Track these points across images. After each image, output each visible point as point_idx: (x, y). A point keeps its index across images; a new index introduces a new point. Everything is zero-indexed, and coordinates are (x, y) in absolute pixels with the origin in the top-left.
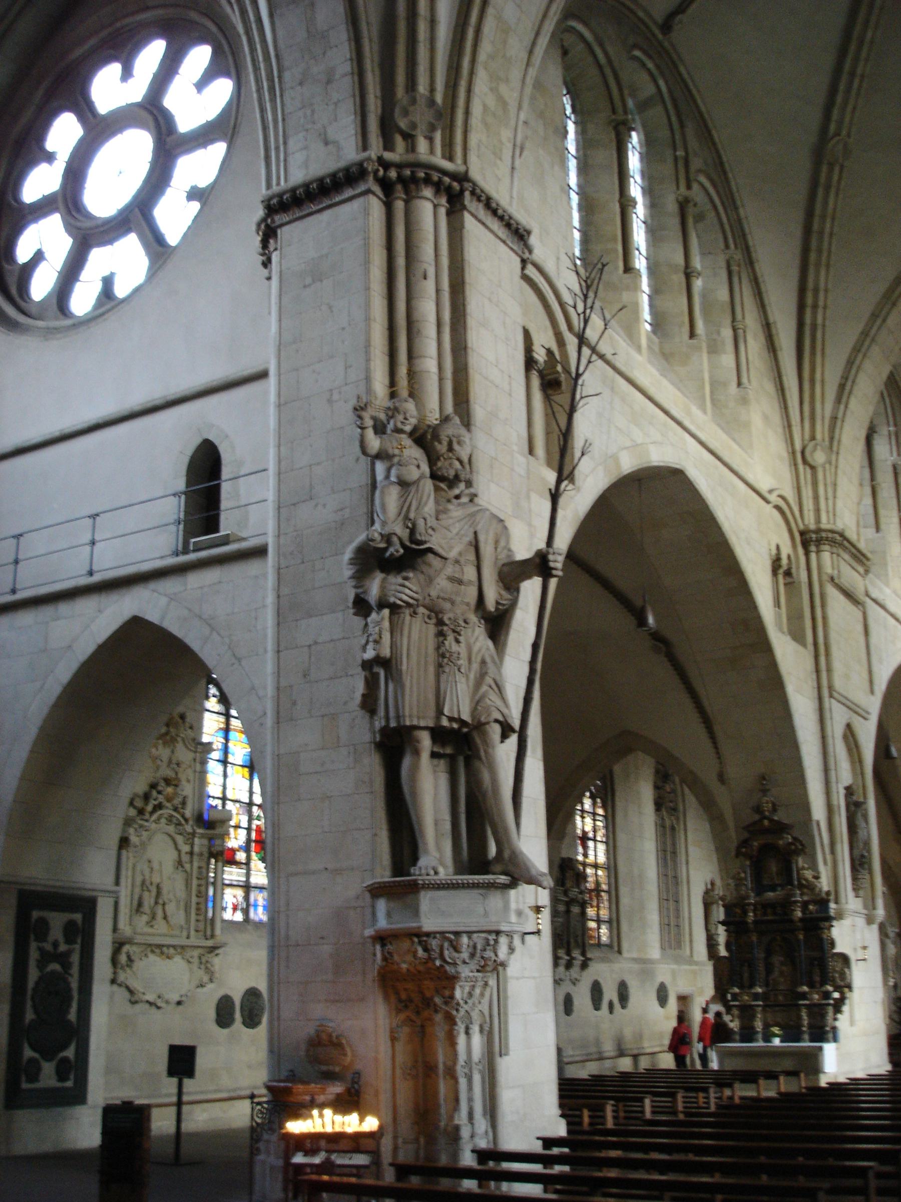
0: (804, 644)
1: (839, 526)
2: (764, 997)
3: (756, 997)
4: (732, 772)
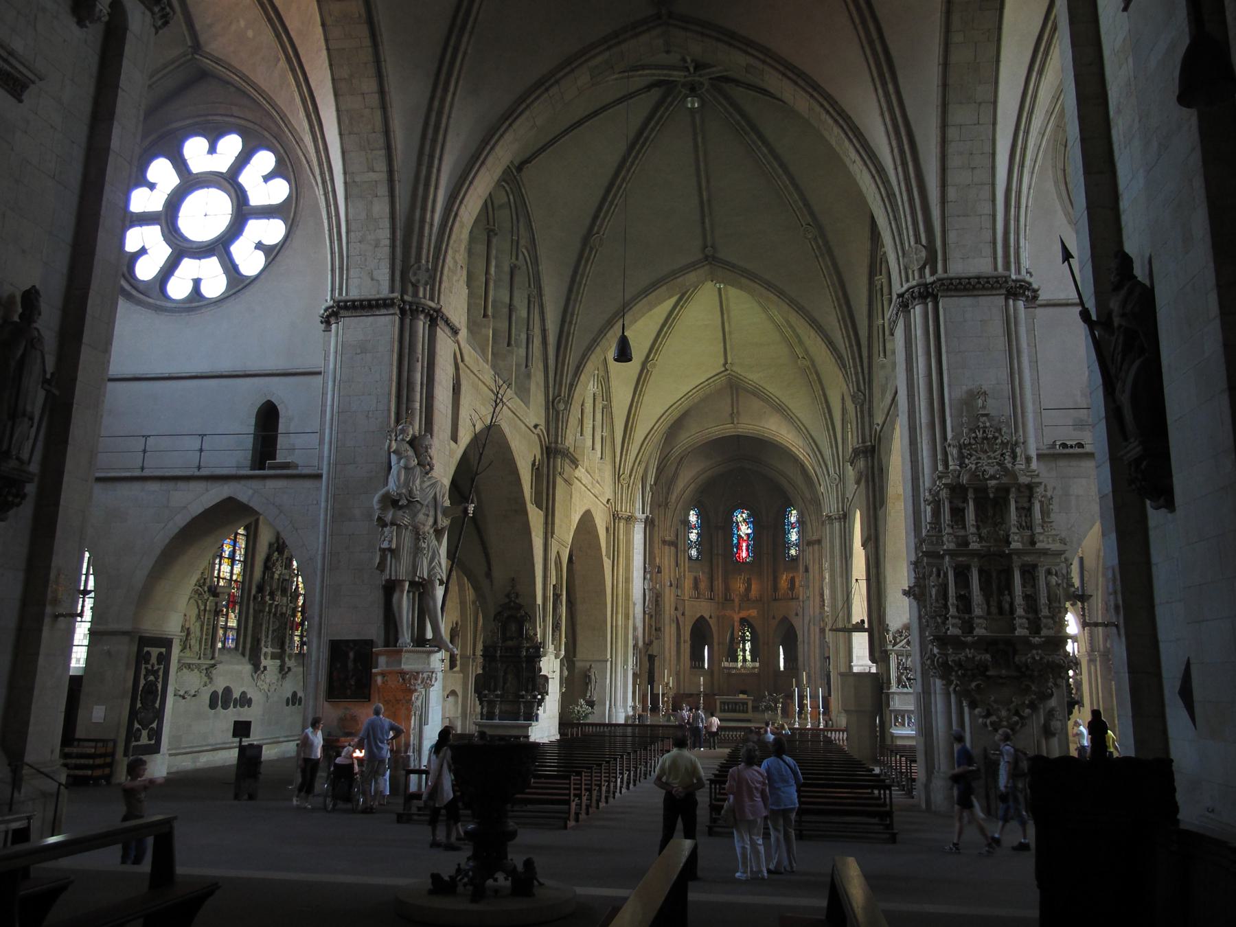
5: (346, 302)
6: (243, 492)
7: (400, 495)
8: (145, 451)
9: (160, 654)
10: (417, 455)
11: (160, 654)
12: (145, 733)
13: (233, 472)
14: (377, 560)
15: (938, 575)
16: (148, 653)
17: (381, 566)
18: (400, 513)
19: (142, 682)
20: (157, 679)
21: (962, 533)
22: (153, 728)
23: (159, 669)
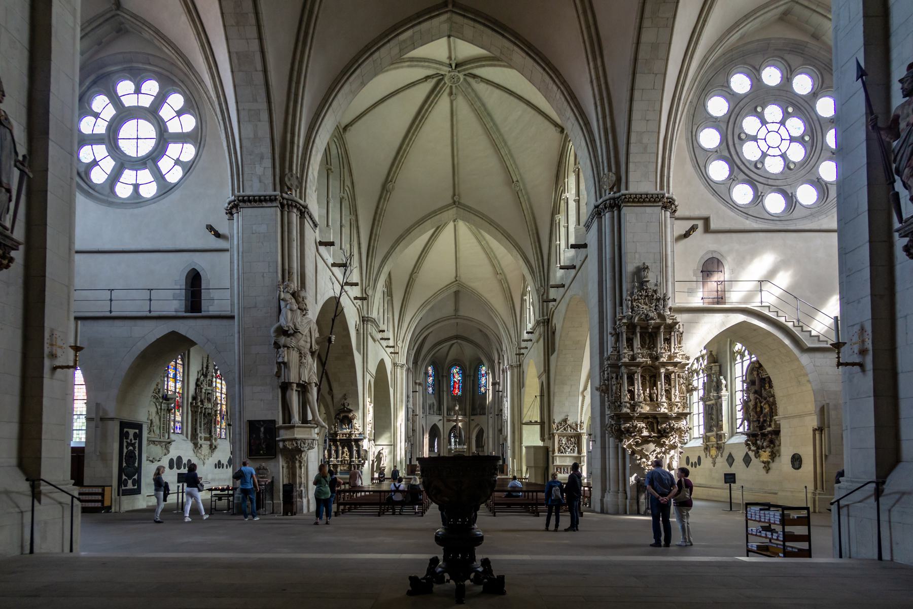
0: (360, 353)
1: (373, 317)
2: (341, 461)
3: (338, 461)
4: (335, 391)
5: (244, 197)
6: (183, 328)
7: (288, 327)
8: (111, 300)
9: (135, 433)
10: (298, 302)
11: (135, 433)
12: (130, 482)
13: (174, 314)
14: (276, 370)
15: (617, 378)
16: (127, 432)
17: (278, 375)
18: (289, 339)
19: (125, 450)
20: (134, 448)
21: (631, 353)
22: (135, 479)
23: (135, 443)
